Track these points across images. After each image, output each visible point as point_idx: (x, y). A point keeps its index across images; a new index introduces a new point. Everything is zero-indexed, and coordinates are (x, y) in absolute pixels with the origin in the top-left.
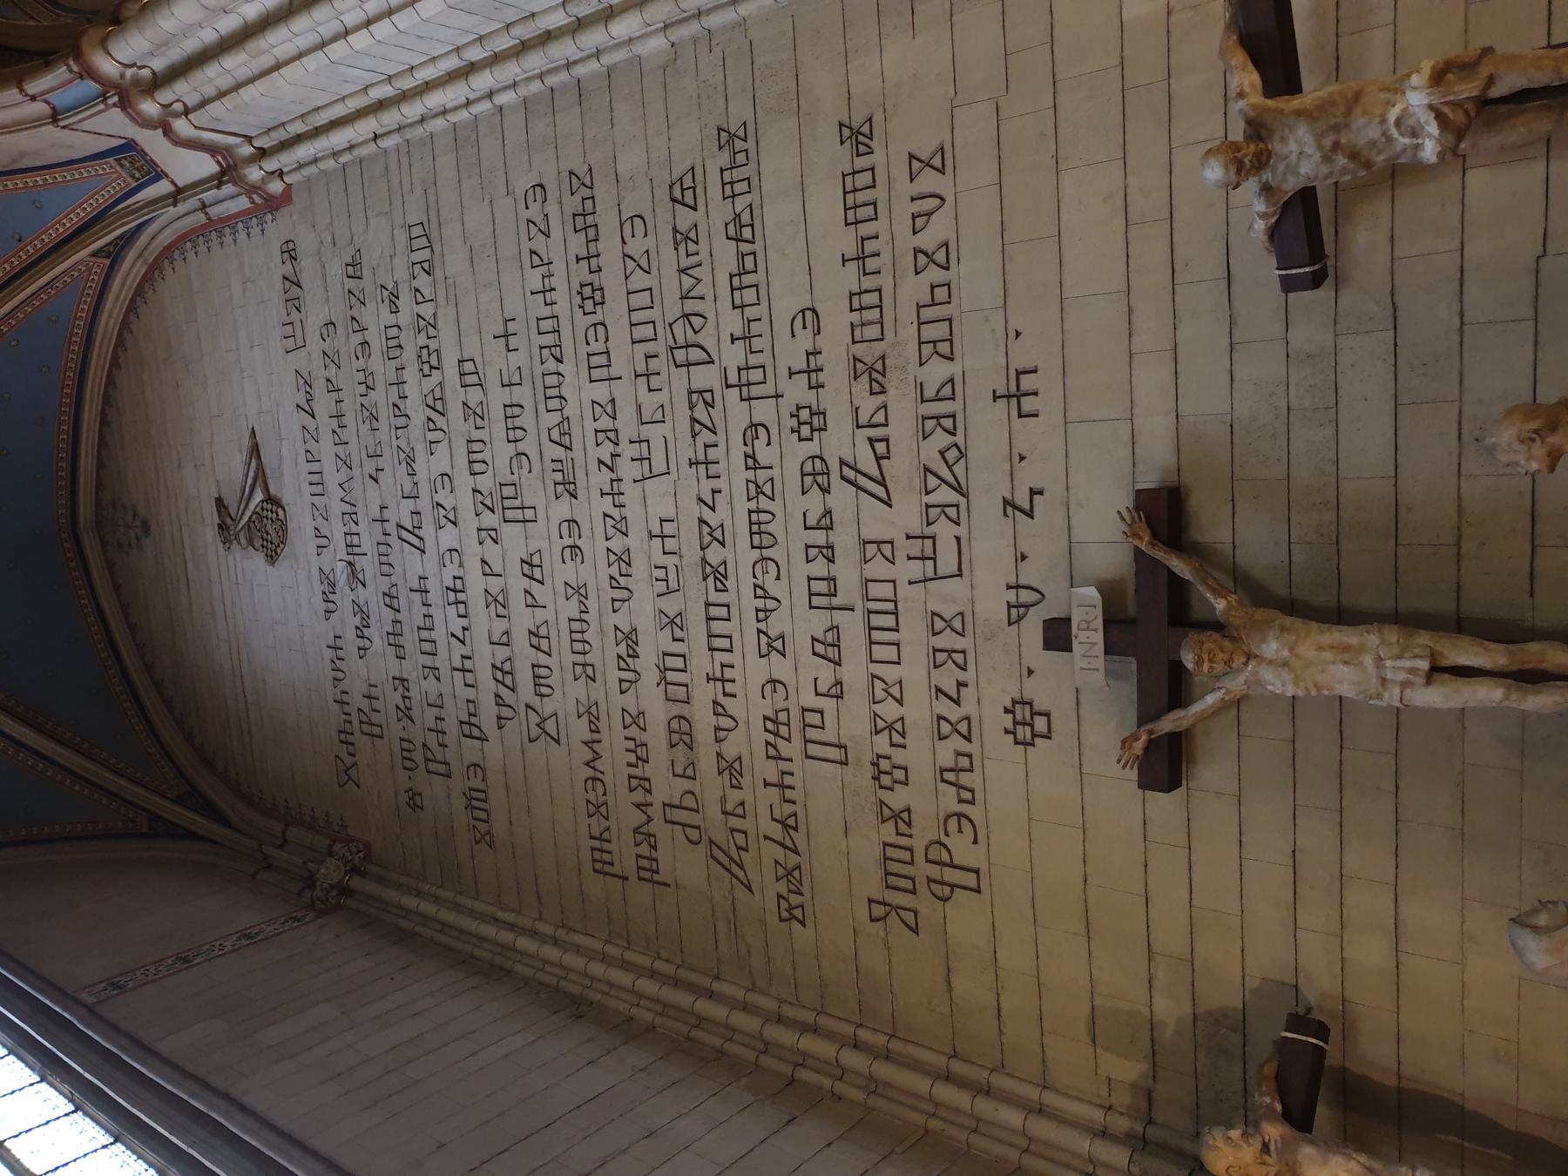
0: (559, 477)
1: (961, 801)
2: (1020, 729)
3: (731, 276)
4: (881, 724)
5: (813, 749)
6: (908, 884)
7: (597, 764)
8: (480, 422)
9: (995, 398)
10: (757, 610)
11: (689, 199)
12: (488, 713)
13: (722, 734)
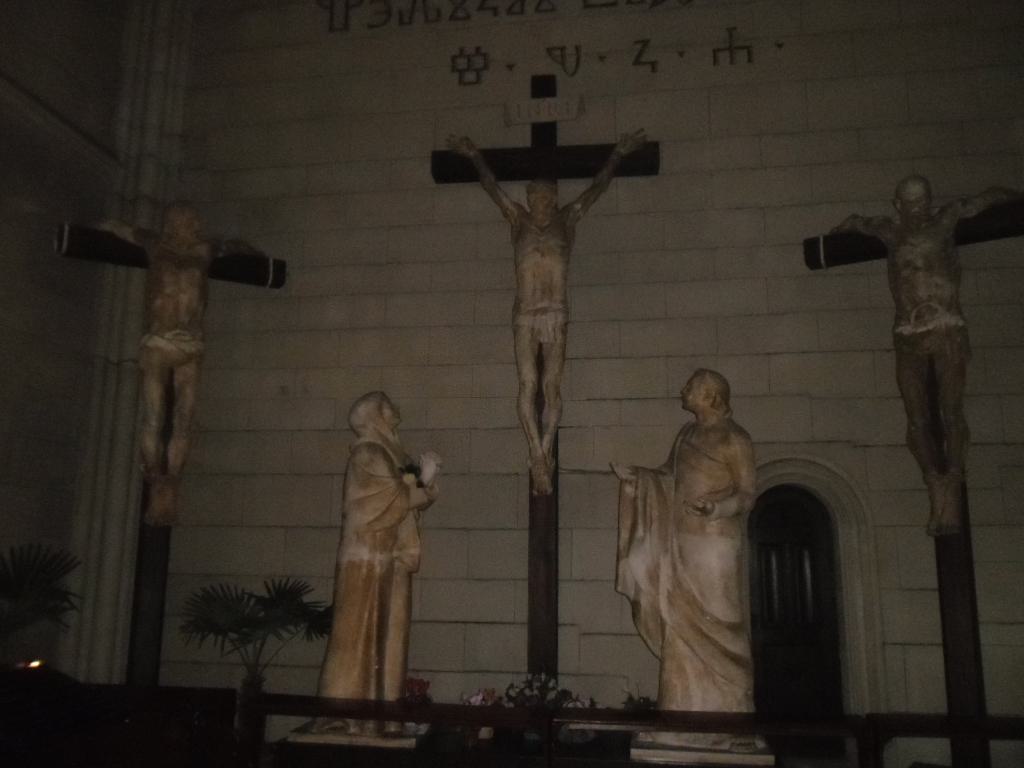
1: (401, 14)
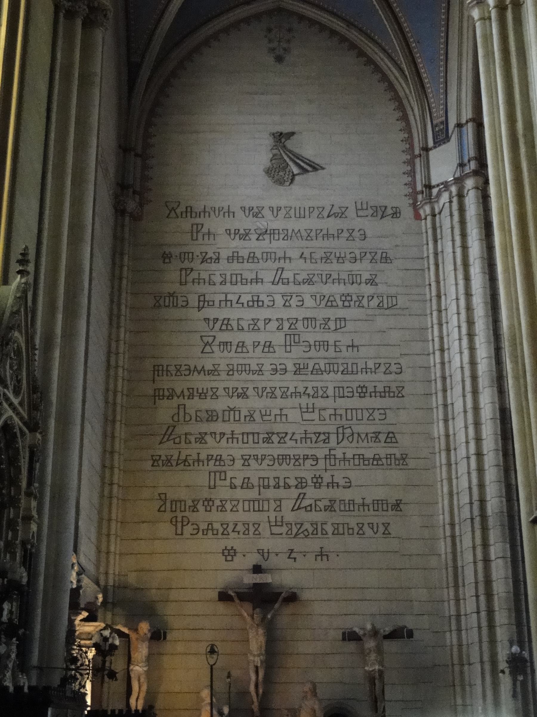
0: (302, 367)
2: (227, 551)
3: (363, 455)
4: (224, 502)
5: (212, 474)
6: (174, 509)
7: (196, 373)
8: (323, 326)
9: (321, 548)
10: (257, 455)
11: (389, 440)
12: (211, 313)
13: (214, 436)
